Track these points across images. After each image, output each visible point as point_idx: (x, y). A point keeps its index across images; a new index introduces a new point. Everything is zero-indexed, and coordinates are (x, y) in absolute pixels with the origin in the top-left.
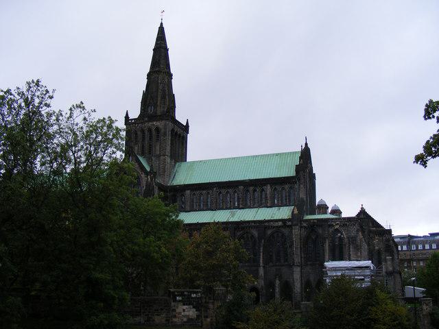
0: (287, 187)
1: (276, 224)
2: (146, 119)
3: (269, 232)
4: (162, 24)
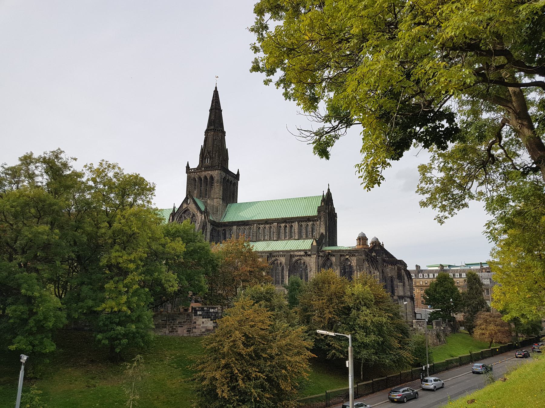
0: (311, 223)
1: (299, 253)
2: (203, 169)
3: (294, 260)
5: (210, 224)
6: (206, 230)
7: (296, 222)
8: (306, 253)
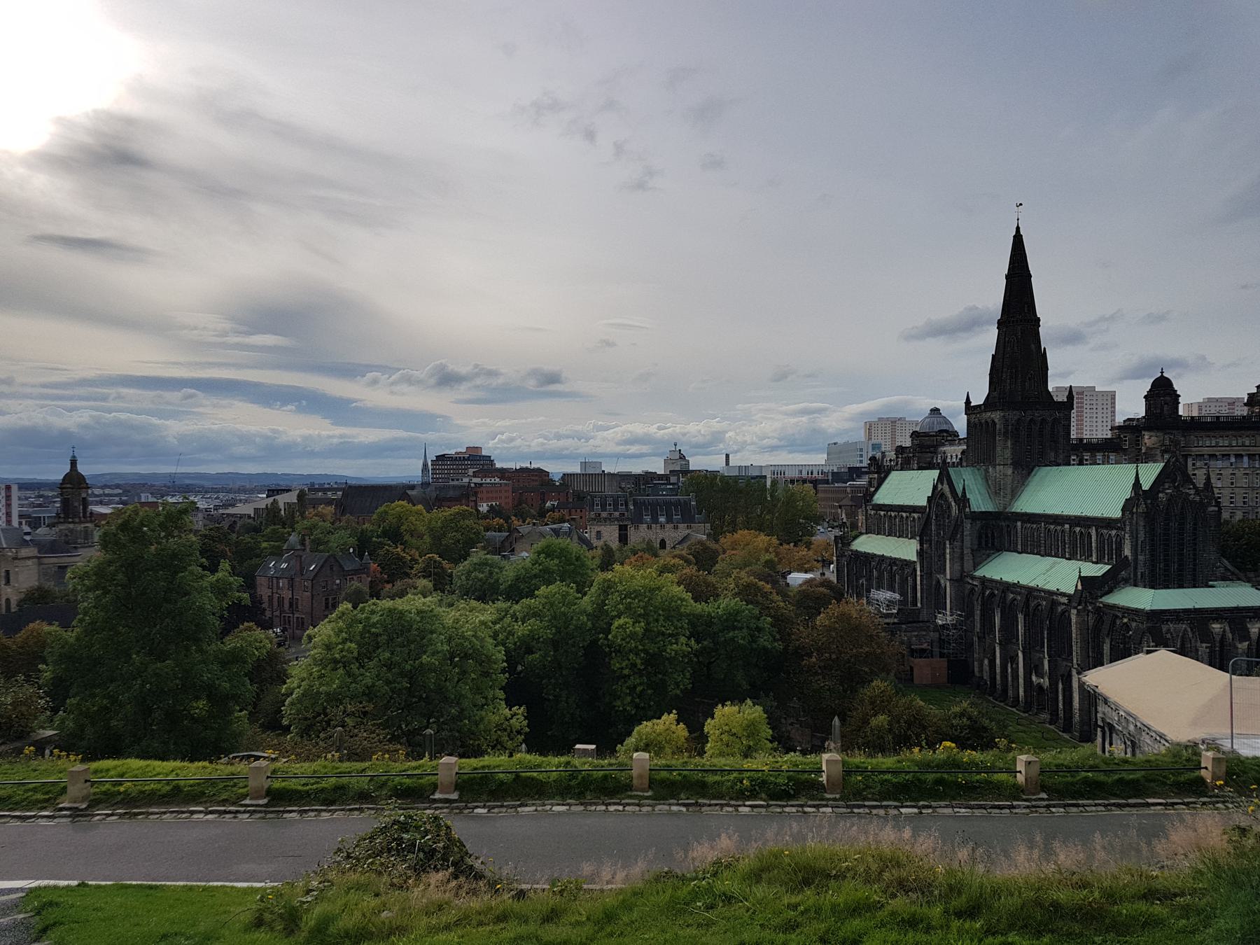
0: (1114, 532)
3: (1060, 609)
6: (963, 532)
7: (1094, 528)
8: (1070, 601)
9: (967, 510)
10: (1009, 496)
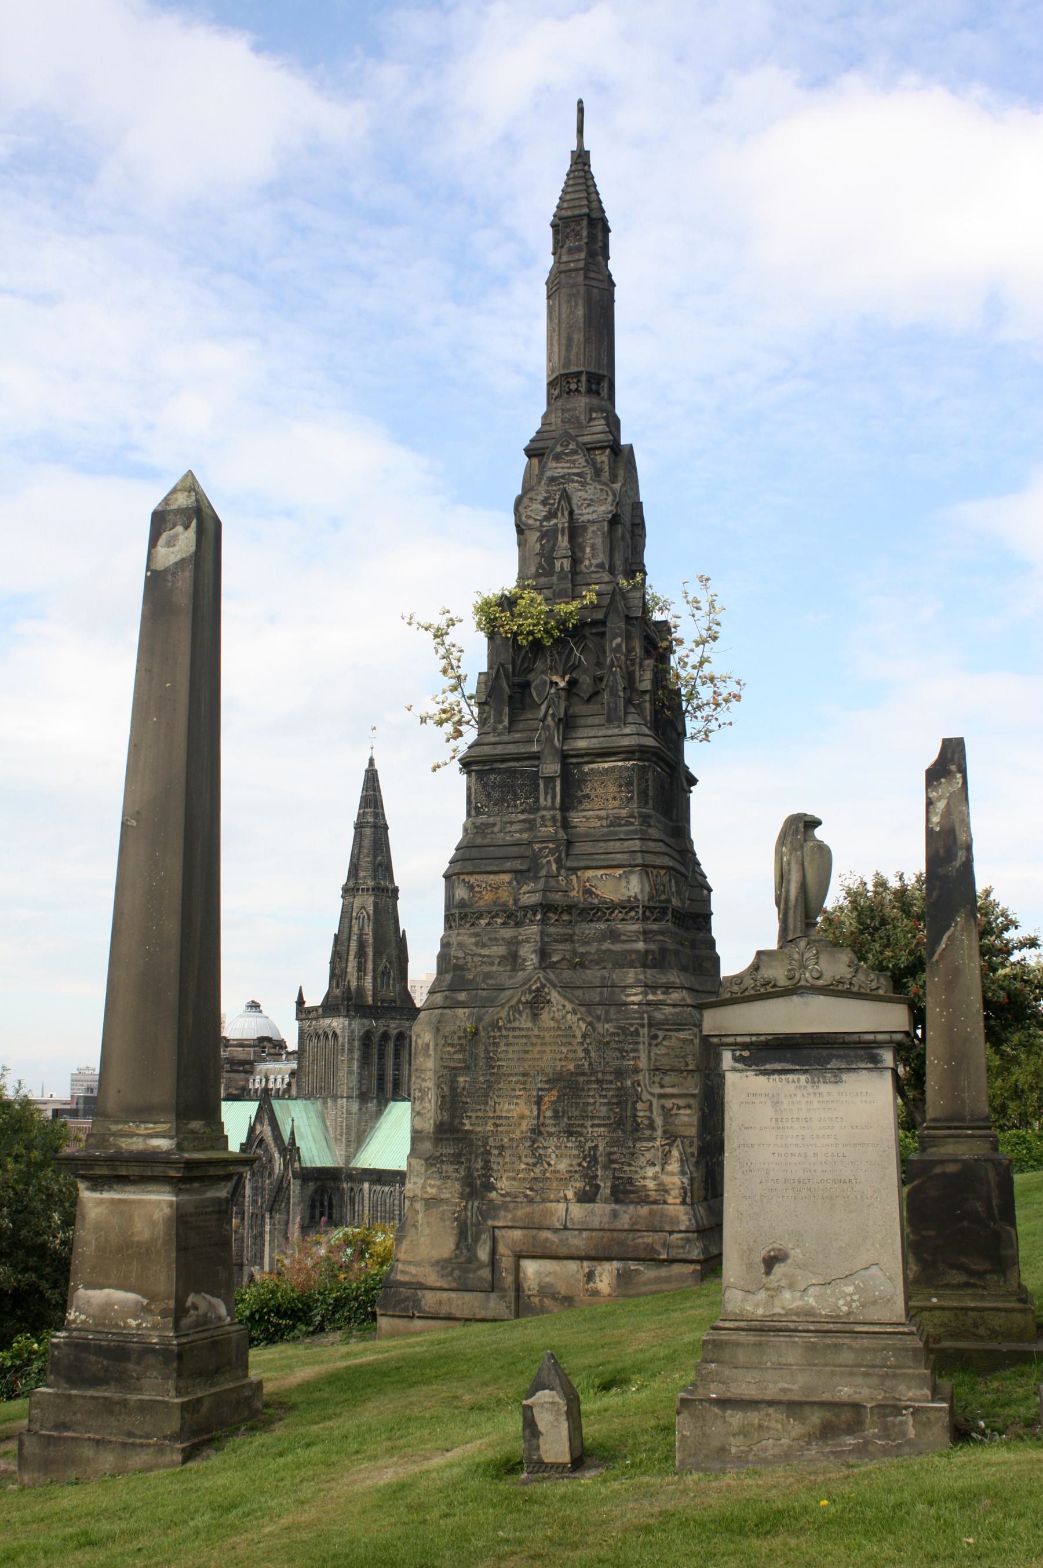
4: (371, 762)
5: (298, 1182)
6: (289, 1199)
9: (297, 1165)
10: (353, 1145)
